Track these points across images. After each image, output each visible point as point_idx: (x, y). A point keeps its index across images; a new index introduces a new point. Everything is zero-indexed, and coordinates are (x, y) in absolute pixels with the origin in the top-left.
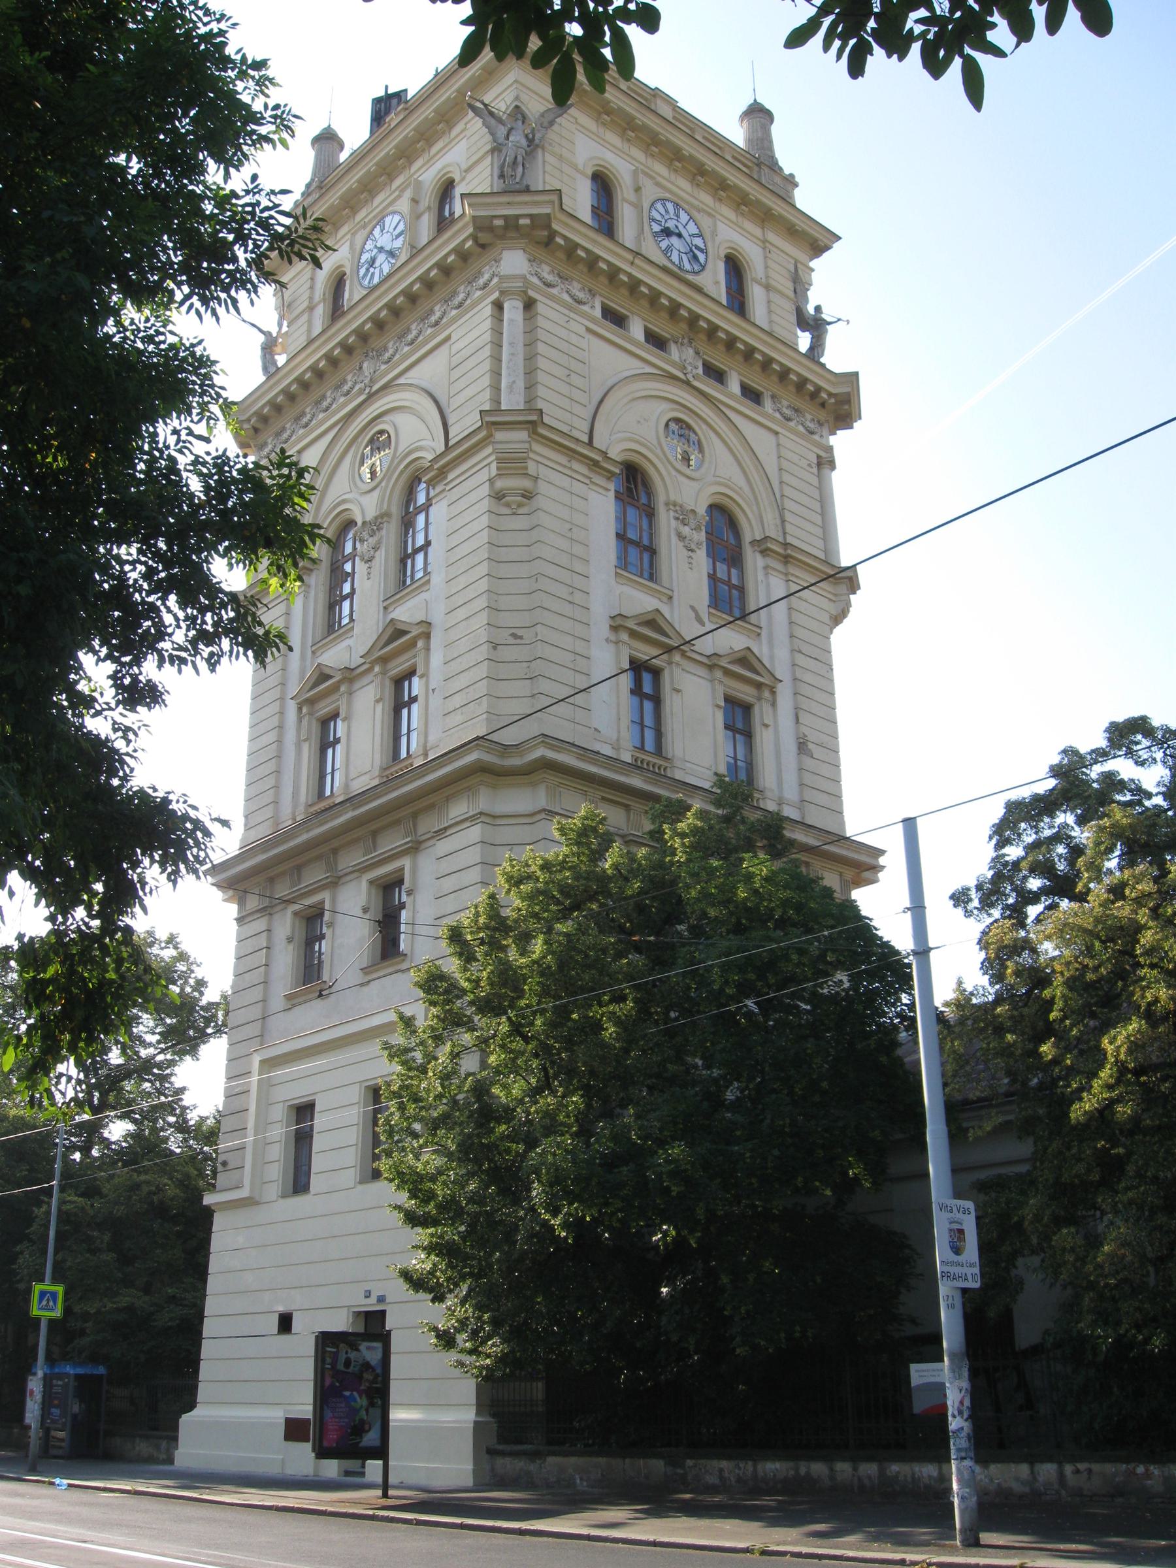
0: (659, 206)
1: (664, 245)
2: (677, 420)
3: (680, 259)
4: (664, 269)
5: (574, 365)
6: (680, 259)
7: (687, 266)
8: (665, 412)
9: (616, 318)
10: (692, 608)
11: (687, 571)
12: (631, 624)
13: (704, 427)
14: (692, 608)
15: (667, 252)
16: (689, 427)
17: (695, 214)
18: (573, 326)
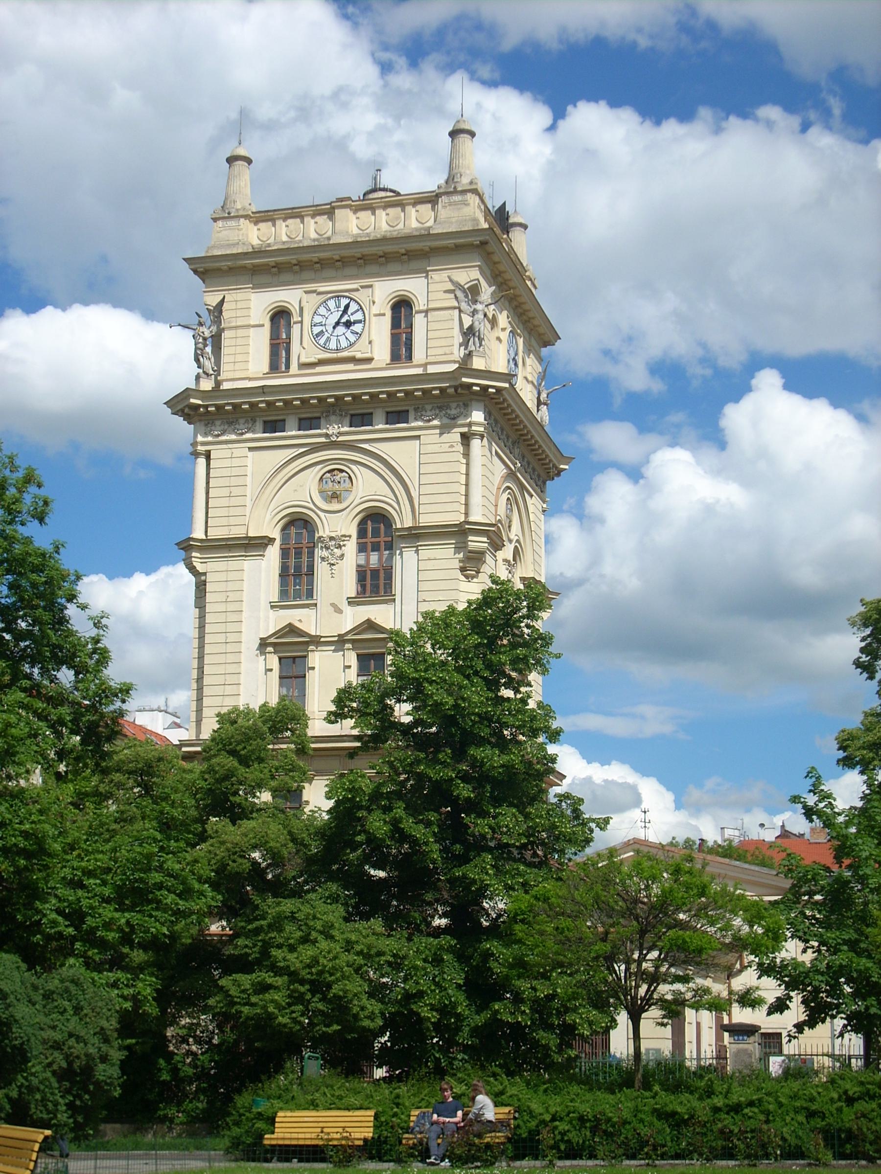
0: (322, 311)
1: (322, 342)
2: (329, 472)
3: (338, 341)
4: (321, 362)
5: (234, 481)
6: (338, 341)
7: (344, 344)
8: (316, 473)
9: (273, 426)
10: (333, 605)
11: (337, 577)
12: (272, 640)
13: (353, 467)
14: (333, 605)
15: (325, 348)
16: (342, 471)
17: (353, 295)
18: (237, 453)
